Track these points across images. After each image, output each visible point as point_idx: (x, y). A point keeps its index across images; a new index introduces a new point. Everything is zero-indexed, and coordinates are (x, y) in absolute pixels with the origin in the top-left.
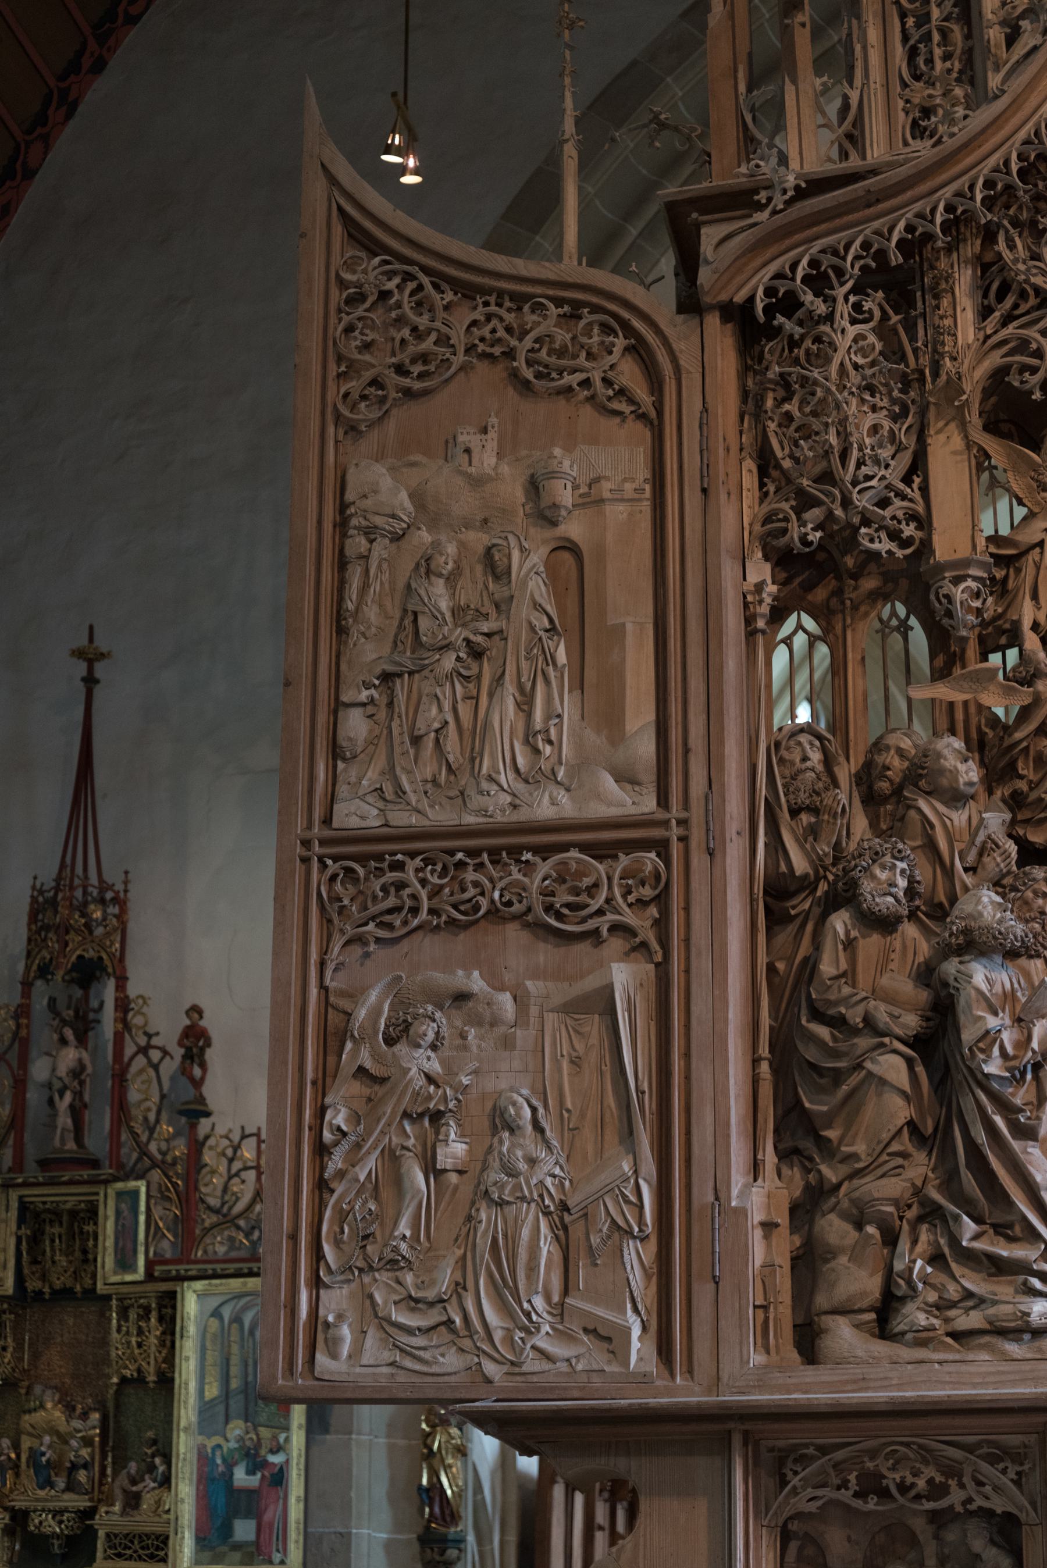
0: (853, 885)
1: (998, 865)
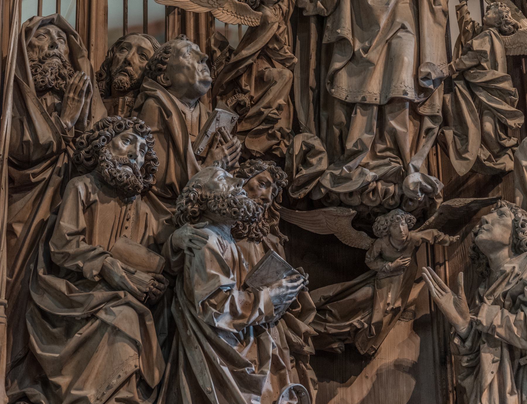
0: (96, 152)
1: (225, 157)
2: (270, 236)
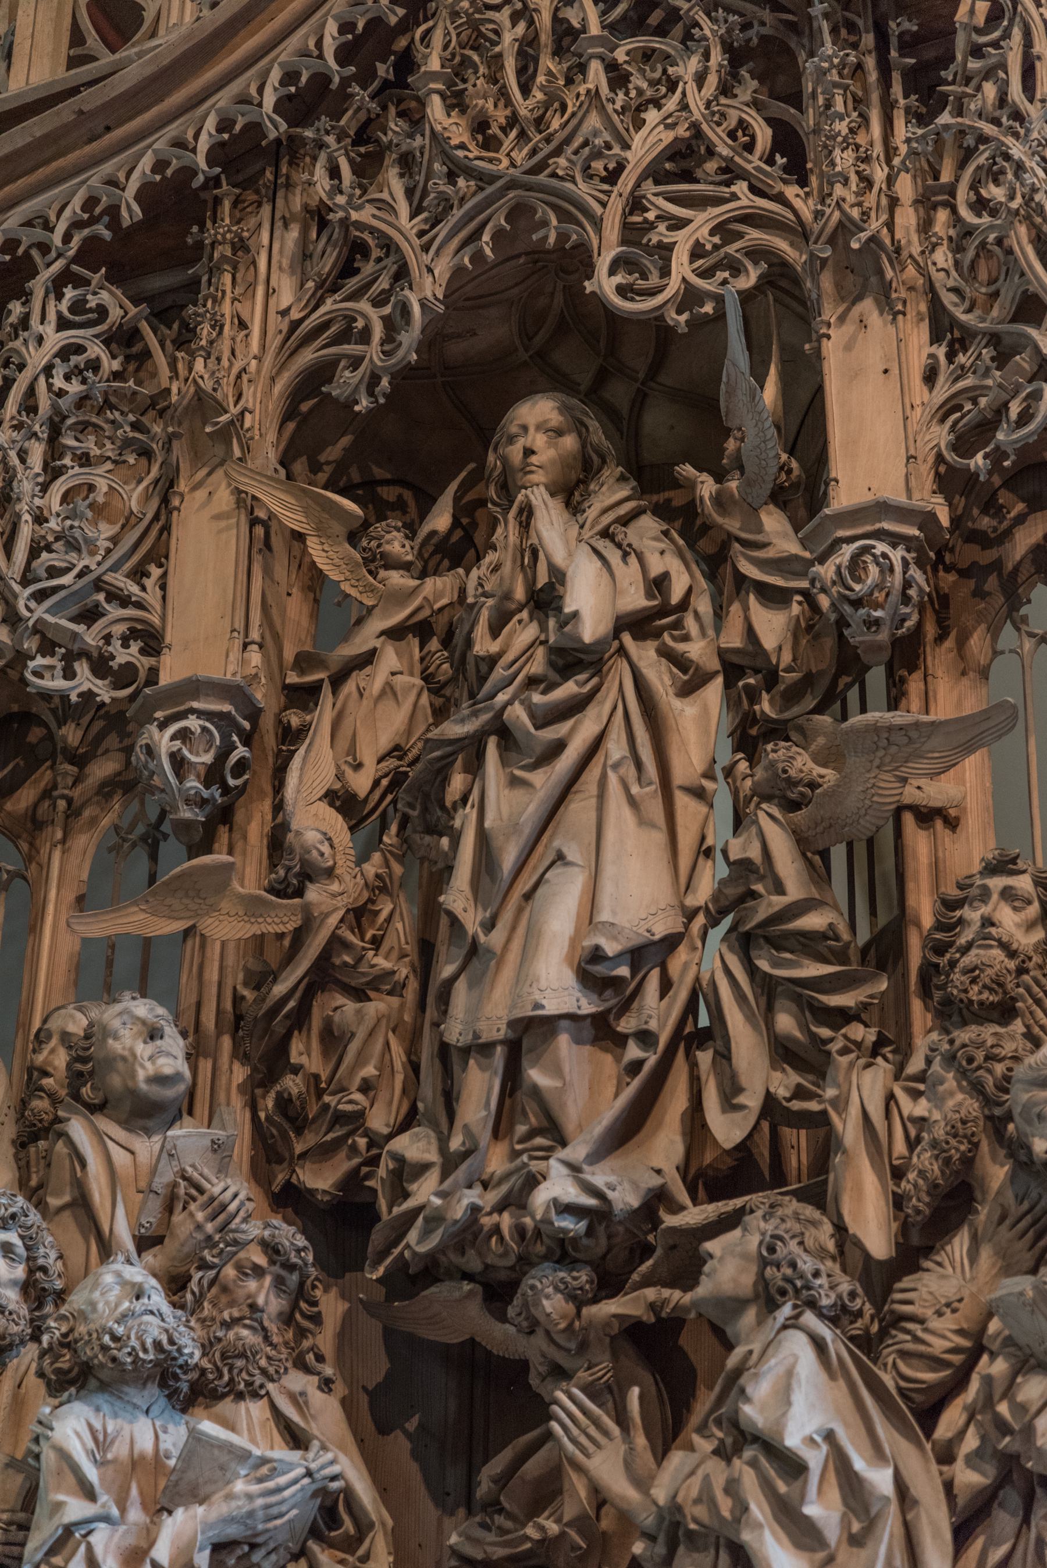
2: (296, 1381)
